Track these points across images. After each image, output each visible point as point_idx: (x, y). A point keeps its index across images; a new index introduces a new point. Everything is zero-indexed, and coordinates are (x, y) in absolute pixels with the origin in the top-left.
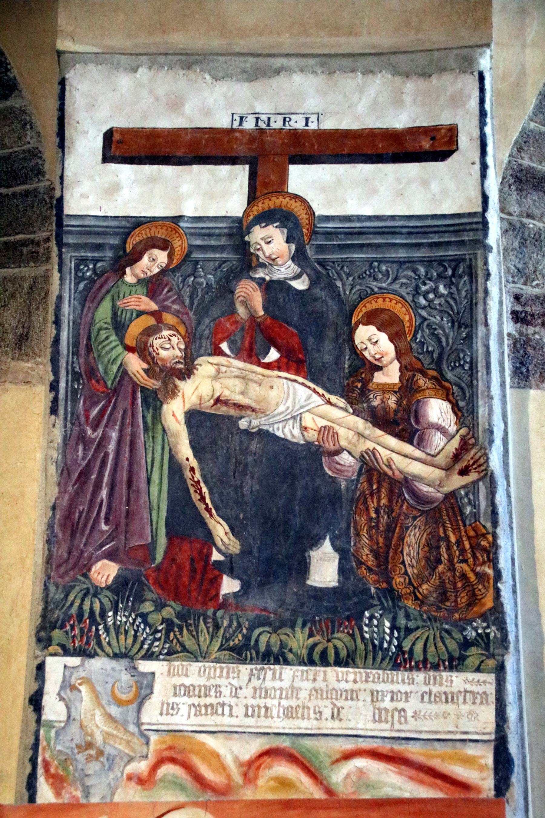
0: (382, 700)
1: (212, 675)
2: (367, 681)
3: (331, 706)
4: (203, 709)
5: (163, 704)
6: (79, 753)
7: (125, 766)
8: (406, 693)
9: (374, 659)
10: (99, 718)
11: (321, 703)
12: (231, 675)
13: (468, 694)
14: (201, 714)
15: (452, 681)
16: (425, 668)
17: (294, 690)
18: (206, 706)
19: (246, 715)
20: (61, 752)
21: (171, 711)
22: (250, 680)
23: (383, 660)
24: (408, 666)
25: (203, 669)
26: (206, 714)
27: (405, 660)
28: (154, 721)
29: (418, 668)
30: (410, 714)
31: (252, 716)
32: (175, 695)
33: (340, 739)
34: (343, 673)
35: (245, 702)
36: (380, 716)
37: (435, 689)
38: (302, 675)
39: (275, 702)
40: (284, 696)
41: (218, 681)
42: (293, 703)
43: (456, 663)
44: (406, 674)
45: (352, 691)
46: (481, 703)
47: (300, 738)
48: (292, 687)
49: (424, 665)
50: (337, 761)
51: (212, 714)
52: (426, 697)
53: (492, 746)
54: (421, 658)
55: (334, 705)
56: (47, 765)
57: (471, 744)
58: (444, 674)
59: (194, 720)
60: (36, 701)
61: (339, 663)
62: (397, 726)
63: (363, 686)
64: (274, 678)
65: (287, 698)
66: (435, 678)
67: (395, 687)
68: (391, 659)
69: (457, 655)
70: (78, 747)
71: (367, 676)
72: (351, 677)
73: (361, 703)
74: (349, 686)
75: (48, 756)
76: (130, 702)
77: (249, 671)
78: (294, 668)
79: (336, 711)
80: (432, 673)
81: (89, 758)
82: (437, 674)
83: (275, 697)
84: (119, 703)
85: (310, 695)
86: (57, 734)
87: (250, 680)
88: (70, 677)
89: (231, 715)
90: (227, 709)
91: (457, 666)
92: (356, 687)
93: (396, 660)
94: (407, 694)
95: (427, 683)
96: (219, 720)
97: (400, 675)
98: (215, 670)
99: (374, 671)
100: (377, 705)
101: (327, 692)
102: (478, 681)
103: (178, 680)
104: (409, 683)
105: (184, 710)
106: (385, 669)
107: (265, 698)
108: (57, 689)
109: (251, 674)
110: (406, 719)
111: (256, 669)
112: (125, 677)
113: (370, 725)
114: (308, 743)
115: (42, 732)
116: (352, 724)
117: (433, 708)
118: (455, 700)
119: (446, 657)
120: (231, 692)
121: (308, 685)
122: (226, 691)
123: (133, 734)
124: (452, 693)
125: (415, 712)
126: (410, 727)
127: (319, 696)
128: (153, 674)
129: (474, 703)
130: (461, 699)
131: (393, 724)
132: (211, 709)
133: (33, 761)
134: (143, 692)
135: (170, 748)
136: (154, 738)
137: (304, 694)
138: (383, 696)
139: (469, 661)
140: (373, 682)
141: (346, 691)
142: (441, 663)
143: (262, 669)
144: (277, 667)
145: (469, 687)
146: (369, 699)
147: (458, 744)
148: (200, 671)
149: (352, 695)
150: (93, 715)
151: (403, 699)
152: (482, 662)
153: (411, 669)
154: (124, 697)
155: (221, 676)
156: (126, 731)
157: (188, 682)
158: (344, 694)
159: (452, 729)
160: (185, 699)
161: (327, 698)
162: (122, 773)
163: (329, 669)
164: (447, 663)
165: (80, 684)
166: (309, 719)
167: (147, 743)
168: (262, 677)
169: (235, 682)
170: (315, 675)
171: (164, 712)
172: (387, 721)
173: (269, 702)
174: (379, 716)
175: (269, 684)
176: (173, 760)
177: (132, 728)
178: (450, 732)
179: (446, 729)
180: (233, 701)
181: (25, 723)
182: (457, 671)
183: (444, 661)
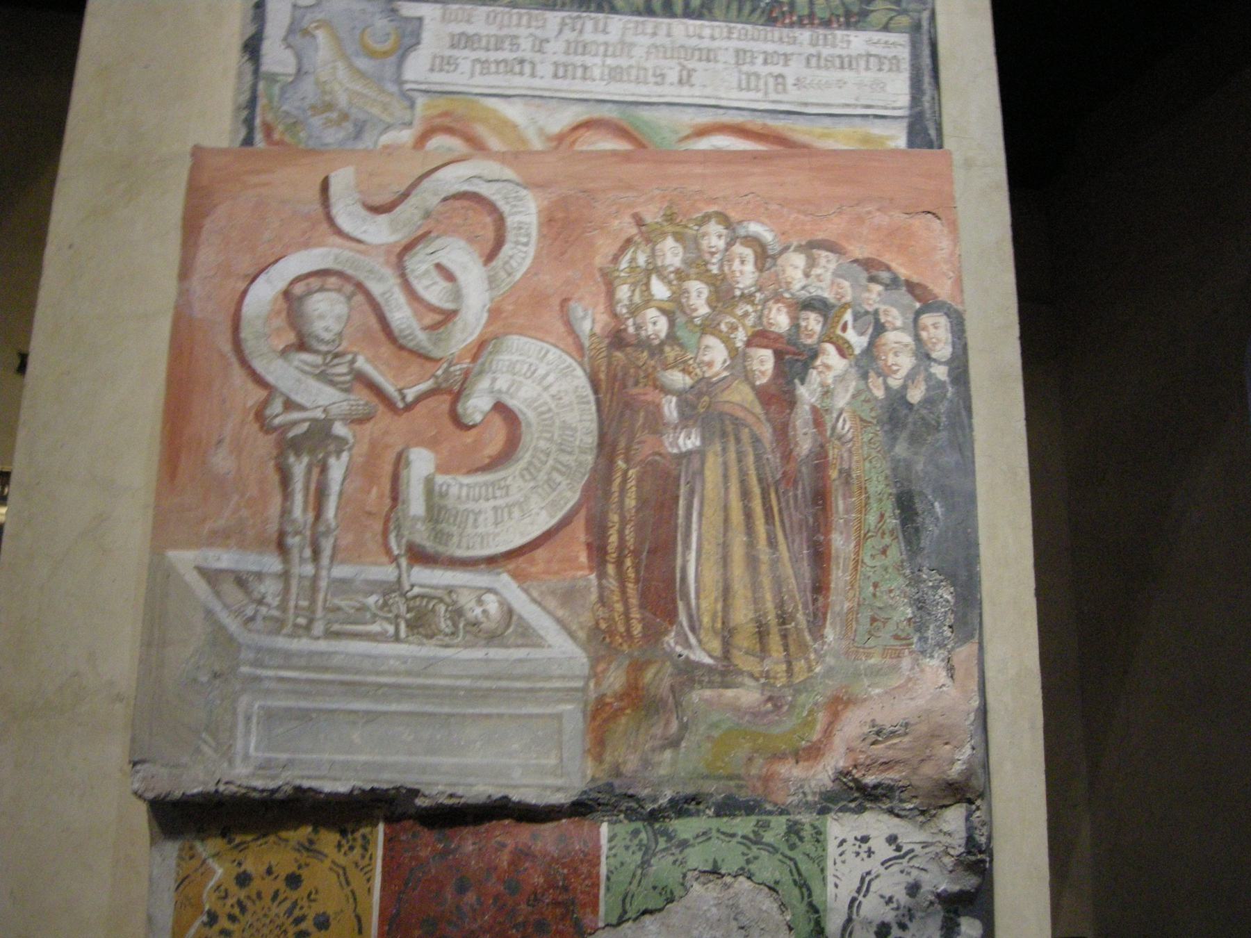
0: (752, 63)
1: (506, 22)
2: (729, 38)
3: (678, 68)
4: (493, 68)
5: (435, 57)
6: (313, 115)
7: (381, 134)
8: (785, 55)
9: (740, 10)
10: (342, 72)
11: (663, 63)
12: (534, 24)
13: (872, 59)
14: (489, 73)
15: (849, 42)
16: (812, 24)
17: (625, 47)
18: (498, 63)
19: (556, 76)
20: (287, 114)
21: (446, 67)
22: (560, 31)
23: (753, 11)
24: (787, 21)
25: (492, 15)
26: (497, 73)
27: (783, 13)
28: (421, 79)
29: (800, 24)
30: (790, 81)
31: (564, 77)
32: (453, 46)
33: (690, 110)
34: (695, 26)
35: (555, 58)
36: (748, 83)
37: (826, 52)
38: (636, 28)
39: (598, 60)
40: (609, 53)
41: (514, 31)
42: (623, 62)
43: (854, 19)
44: (786, 31)
45: (709, 50)
46: (890, 70)
47: (632, 107)
48: (622, 42)
49: (809, 20)
50: (687, 137)
51: (506, 72)
52: (813, 61)
53: (904, 124)
54: (806, 12)
55: (684, 67)
56: (268, 130)
57: (877, 121)
58: (839, 33)
59: (478, 80)
60: (252, 48)
61: (688, 13)
62: (773, 96)
63: (725, 44)
64: (596, 30)
65: (614, 55)
66: (825, 36)
67: (770, 47)
68: (763, 12)
69: (855, 9)
70: (313, 107)
71: (730, 32)
72: (707, 32)
73: (720, 66)
74: (706, 43)
75: (270, 117)
76: (386, 54)
77: (558, 20)
78: (626, 18)
79: (685, 73)
80: (821, 31)
81: (328, 123)
82: (828, 32)
83: (596, 55)
84: (372, 54)
85: (648, 53)
86: (283, 91)
87: (560, 31)
88: (303, 16)
89: (533, 75)
90: (527, 68)
91: (857, 22)
92: (716, 44)
93: (771, 12)
94: (787, 57)
95: (814, 44)
96: (517, 81)
97: (776, 32)
98: (511, 16)
99: (740, 26)
100: (745, 68)
101: (673, 49)
102: (886, 42)
103: (457, 28)
104: (789, 43)
105: (465, 66)
106: (755, 24)
107: (583, 54)
108: (282, 33)
109: (563, 24)
110: (784, 85)
111: (570, 17)
112: (381, 23)
113: (735, 94)
114: (646, 114)
115: (261, 86)
116: (708, 91)
117: (823, 74)
118: (854, 65)
119: (841, 11)
120: (534, 46)
121: (645, 41)
122: (526, 44)
123: (392, 94)
124: (850, 56)
125: (798, 79)
126: (791, 98)
127: (661, 55)
128: (420, 19)
129: (880, 70)
130: (862, 63)
131: (766, 93)
132: (508, 67)
133: (249, 122)
134: (408, 41)
135: (446, 114)
136: (421, 101)
137: (638, 52)
138: (753, 57)
139: (873, 18)
140: (739, 39)
141: (700, 49)
142: (834, 19)
143: (579, 17)
144: (601, 16)
145: (874, 50)
146: (733, 61)
147: (857, 120)
148: (488, 16)
149: (708, 56)
150: (335, 68)
151: (782, 62)
152: (891, 19)
153: (792, 25)
154: (379, 47)
155: (519, 25)
156: (382, 91)
157: (470, 30)
158: (697, 53)
159: (853, 102)
160: (466, 53)
161: (672, 57)
162: (376, 143)
163: (674, 21)
164: (842, 19)
165: (317, 28)
166: (646, 83)
167: (412, 106)
168: (578, 27)
169: (538, 33)
170: (656, 27)
171: (437, 67)
172: (758, 90)
173: (589, 60)
174: (749, 82)
175: (588, 36)
176: (449, 131)
177: (391, 87)
178: (848, 105)
179: (843, 101)
180: (537, 57)
181: (240, 75)
182: (857, 29)
183: (838, 16)
